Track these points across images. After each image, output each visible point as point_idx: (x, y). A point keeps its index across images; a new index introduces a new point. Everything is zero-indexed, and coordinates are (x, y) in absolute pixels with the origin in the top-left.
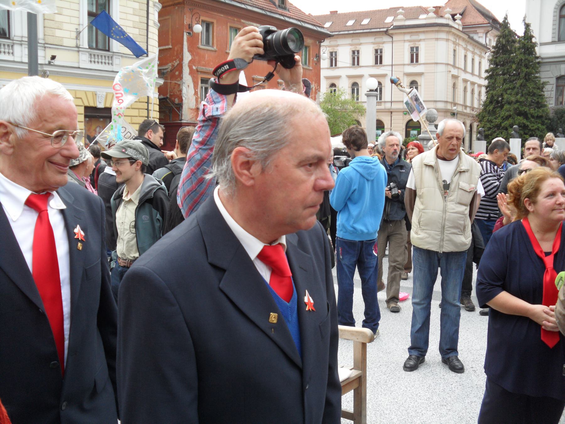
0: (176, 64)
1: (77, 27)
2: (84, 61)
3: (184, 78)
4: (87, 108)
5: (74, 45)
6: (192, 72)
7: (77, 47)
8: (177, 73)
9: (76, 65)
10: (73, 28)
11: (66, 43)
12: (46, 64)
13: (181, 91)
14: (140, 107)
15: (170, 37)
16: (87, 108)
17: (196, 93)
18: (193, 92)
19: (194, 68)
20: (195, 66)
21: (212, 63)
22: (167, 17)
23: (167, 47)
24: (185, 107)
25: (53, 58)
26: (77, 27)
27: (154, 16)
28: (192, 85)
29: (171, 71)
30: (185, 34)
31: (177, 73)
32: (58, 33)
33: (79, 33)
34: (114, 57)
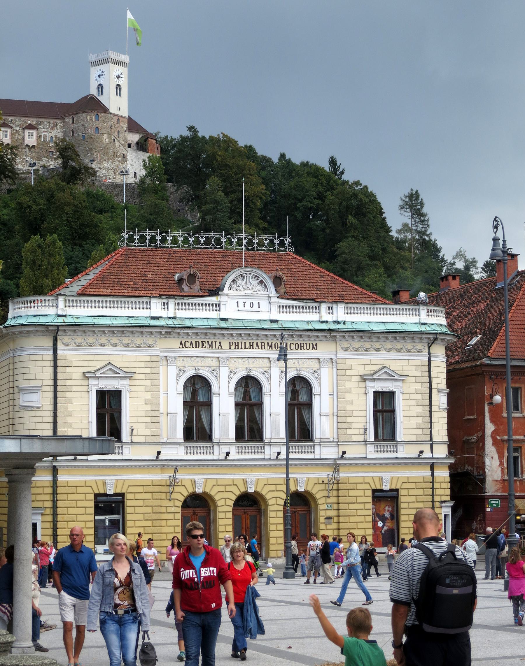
0: (480, 435)
1: (365, 424)
2: (371, 452)
3: (486, 450)
4: (374, 491)
5: (362, 439)
6: (495, 443)
7: (365, 441)
8: (481, 444)
9: (364, 456)
10: (361, 425)
11: (355, 439)
12: (338, 459)
13: (484, 463)
14: (424, 487)
15: (475, 407)
16: (374, 491)
17: (501, 464)
18: (498, 463)
19: (498, 438)
20: (499, 435)
21: (520, 431)
22: (473, 386)
23: (472, 417)
24: (489, 480)
25: (344, 453)
26: (365, 424)
27: (441, 401)
28: (496, 456)
29: (477, 442)
30: (486, 405)
31: (481, 444)
32: (349, 432)
33: (366, 430)
34: (398, 445)
